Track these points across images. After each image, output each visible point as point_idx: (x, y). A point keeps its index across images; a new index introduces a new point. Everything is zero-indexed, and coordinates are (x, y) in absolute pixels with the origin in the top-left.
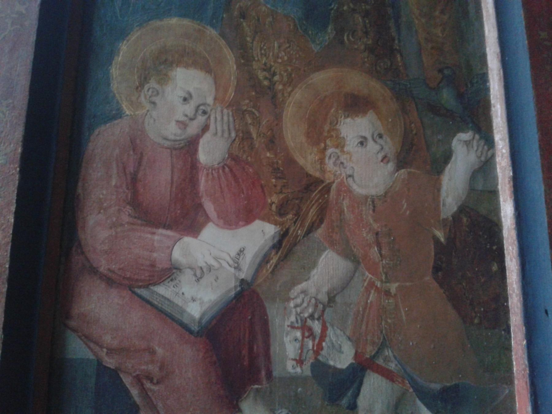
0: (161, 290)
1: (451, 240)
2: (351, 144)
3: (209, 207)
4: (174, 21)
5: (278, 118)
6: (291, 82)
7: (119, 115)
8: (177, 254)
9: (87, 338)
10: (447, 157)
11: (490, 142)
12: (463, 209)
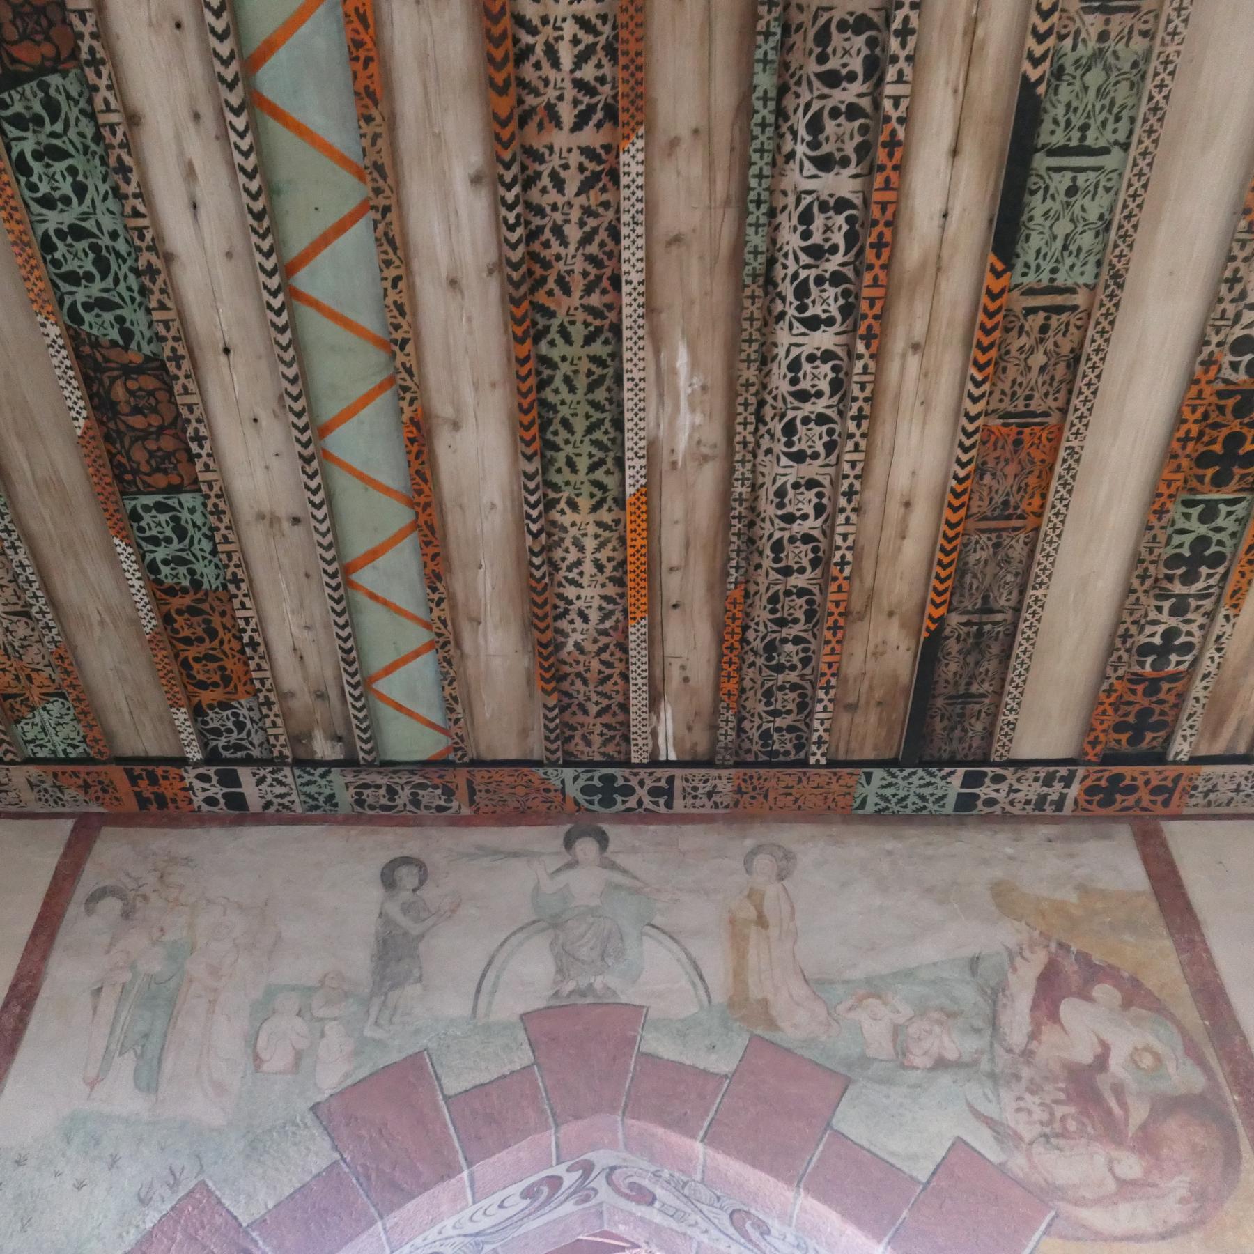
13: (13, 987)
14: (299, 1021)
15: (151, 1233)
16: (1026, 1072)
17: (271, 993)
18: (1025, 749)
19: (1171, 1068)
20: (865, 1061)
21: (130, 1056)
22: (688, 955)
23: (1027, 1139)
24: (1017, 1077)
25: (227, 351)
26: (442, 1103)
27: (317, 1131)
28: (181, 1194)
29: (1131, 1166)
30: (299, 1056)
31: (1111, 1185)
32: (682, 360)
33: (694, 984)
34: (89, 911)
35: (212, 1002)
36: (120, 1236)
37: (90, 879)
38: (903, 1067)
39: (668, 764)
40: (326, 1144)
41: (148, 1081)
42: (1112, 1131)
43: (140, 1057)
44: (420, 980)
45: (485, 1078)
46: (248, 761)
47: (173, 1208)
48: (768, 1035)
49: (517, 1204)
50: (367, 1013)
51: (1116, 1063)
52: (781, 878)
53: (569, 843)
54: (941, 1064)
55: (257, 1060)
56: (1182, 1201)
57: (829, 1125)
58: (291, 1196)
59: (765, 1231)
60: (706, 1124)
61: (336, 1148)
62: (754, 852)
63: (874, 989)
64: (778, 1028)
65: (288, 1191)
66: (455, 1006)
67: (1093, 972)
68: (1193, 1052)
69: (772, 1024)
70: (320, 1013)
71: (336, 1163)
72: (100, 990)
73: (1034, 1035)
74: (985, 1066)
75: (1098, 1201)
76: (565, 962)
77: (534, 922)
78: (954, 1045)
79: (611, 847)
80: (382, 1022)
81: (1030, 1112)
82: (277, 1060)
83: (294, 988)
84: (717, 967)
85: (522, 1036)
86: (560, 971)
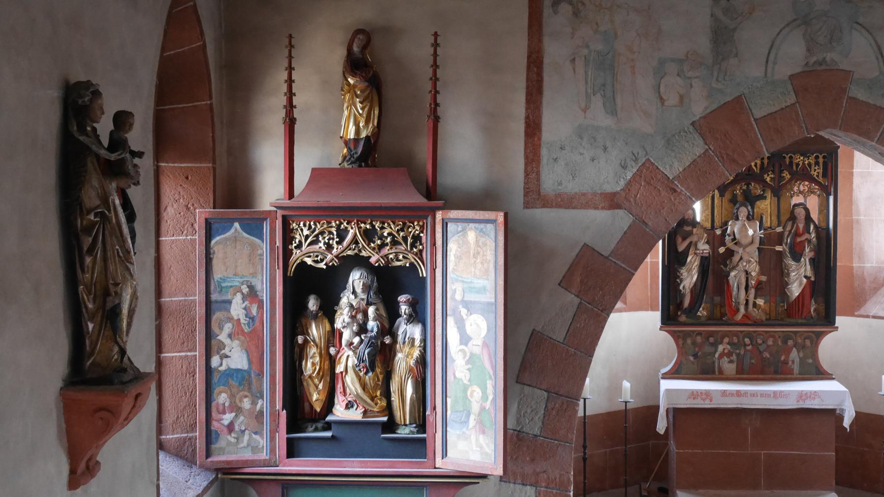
0: (222, 422)
1: (257, 414)
2: (245, 402)
3: (227, 411)
4: (221, 387)
5: (235, 400)
6: (237, 394)
7: (215, 400)
8: (223, 417)
9: (214, 427)
10: (258, 403)
11: (264, 401)
12: (259, 410)
13: (529, 57)
14: (678, 78)
15: (630, 181)
17: (662, 62)
21: (598, 95)
26: (754, 123)
27: (696, 136)
28: (640, 164)
30: (681, 97)
33: (877, 58)
34: (556, 12)
35: (633, 67)
36: (617, 182)
40: (701, 142)
41: (612, 111)
43: (604, 96)
44: (736, 55)
45: (774, 109)
47: (638, 170)
50: (712, 75)
58: (689, 166)
60: (879, 135)
61: (706, 144)
65: (687, 164)
66: (758, 72)
70: (690, 74)
71: (707, 150)
72: (574, 59)
77: (795, 20)
80: (720, 79)
83: (673, 60)
85: (790, 88)
86: (808, 50)
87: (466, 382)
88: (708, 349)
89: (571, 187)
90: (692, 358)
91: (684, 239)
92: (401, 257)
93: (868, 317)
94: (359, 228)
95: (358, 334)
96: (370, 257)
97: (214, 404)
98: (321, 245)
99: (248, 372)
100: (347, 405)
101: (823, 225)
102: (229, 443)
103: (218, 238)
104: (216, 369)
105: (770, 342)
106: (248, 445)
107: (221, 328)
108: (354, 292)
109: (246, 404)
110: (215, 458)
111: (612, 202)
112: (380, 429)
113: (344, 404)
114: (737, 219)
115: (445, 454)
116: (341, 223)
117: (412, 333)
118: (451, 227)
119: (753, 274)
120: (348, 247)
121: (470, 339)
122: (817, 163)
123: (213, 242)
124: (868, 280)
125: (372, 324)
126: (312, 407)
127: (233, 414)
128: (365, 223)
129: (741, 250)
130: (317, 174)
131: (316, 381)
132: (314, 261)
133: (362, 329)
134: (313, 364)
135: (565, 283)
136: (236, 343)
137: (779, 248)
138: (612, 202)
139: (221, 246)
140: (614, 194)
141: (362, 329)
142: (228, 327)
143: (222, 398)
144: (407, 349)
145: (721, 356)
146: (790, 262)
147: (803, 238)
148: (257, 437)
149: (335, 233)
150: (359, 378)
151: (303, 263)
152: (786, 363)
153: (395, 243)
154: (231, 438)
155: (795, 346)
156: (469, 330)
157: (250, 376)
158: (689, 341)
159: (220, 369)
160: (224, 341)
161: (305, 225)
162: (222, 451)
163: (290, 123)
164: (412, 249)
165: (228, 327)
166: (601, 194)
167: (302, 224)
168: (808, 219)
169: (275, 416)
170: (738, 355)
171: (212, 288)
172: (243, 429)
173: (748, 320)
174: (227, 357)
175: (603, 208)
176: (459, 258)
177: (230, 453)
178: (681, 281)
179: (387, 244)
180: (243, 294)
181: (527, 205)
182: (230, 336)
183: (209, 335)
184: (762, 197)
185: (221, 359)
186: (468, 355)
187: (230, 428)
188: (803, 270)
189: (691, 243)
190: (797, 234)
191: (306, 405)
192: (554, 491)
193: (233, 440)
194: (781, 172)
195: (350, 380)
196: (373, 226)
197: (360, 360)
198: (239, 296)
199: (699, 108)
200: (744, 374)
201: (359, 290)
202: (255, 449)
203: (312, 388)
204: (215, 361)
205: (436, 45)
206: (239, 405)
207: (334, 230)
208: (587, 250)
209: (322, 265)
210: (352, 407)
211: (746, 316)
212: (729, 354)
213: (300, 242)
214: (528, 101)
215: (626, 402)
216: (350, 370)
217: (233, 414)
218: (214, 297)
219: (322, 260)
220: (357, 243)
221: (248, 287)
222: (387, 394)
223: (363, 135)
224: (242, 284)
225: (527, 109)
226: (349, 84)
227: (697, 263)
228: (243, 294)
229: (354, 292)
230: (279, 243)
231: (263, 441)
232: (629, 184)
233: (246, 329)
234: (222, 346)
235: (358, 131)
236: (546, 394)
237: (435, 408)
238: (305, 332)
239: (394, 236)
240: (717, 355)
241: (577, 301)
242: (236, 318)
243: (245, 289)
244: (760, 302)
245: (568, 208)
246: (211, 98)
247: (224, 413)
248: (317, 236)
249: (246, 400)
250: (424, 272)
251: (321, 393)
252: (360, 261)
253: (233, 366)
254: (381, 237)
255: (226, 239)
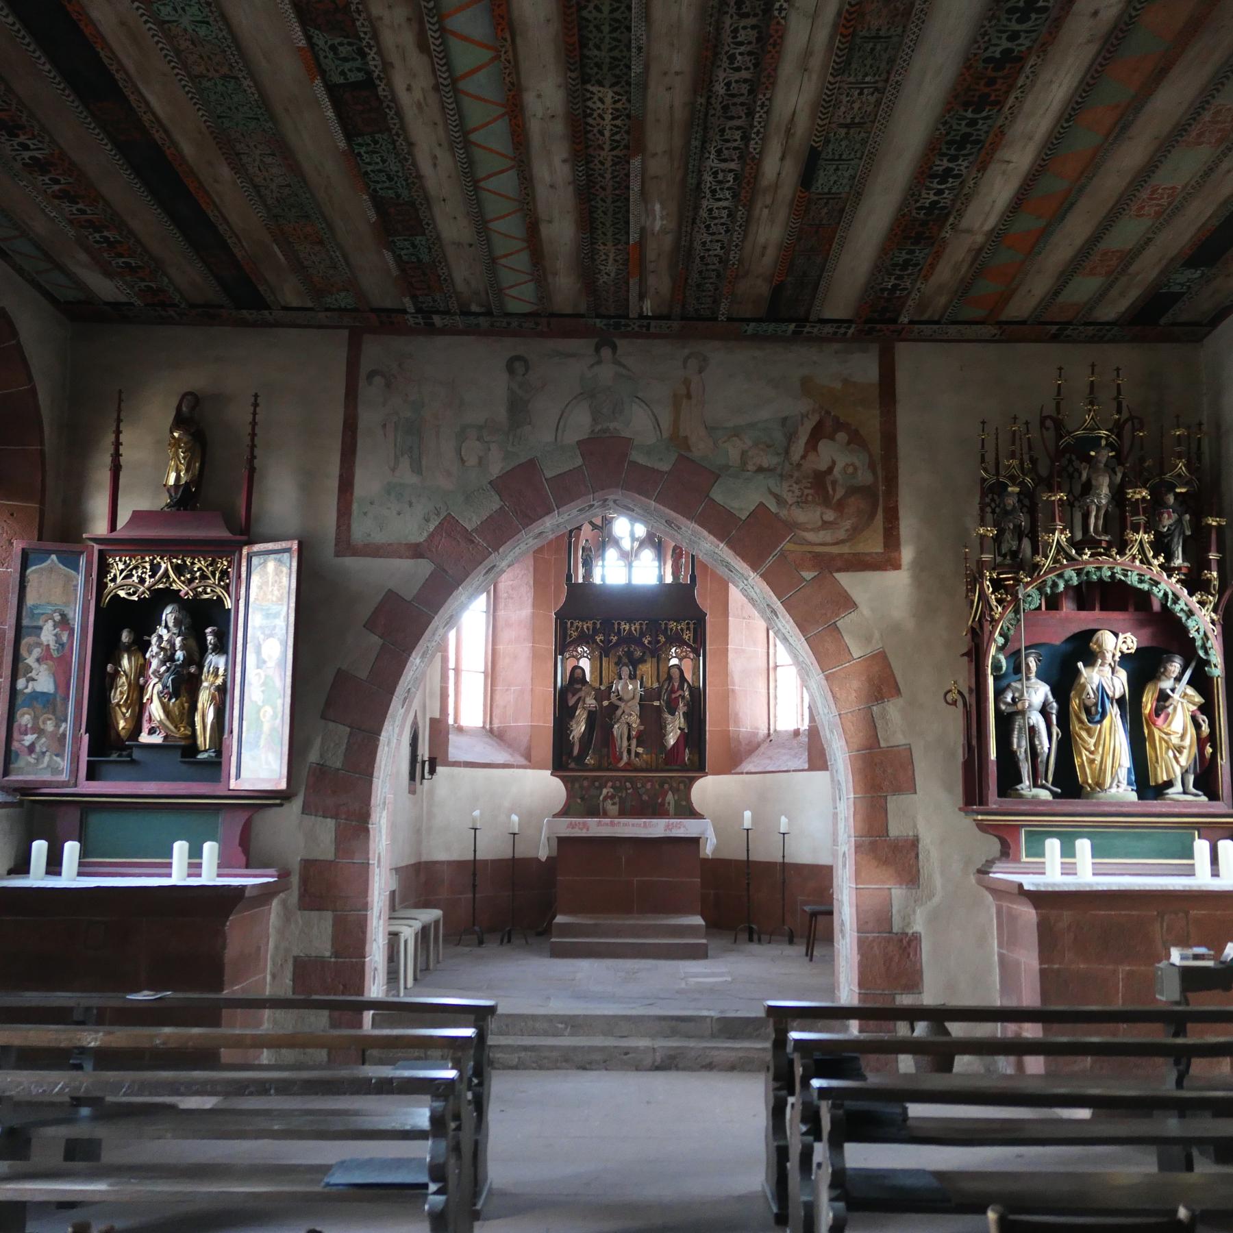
14: (477, 442)
16: (796, 474)
18: (827, 315)
19: (860, 473)
20: (727, 467)
21: (406, 456)
22: (652, 412)
23: (790, 502)
24: (791, 476)
25: (444, 200)
29: (830, 516)
30: (480, 459)
31: (820, 523)
32: (658, 207)
37: (365, 367)
38: (743, 470)
39: (647, 317)
40: (497, 498)
41: (417, 469)
42: (826, 501)
46: (437, 312)
48: (685, 454)
49: (575, 512)
51: (836, 470)
52: (700, 372)
53: (597, 349)
54: (760, 470)
55: (463, 461)
56: (847, 530)
57: (708, 496)
59: (680, 528)
62: (688, 357)
63: (736, 432)
64: (691, 451)
66: (548, 437)
67: (839, 426)
68: (872, 466)
69: (689, 449)
73: (804, 457)
74: (779, 471)
75: (812, 530)
76: (596, 416)
78: (767, 460)
79: (619, 352)
81: (793, 492)
82: (472, 461)
84: (666, 420)
85: (578, 452)
86: (594, 420)
87: (260, 703)
88: (593, 792)
89: (379, 538)
90: (579, 801)
91: (574, 695)
92: (209, 590)
93: (742, 773)
94: (171, 563)
95: (163, 663)
96: (180, 590)
97: (16, 725)
98: (135, 578)
99: (54, 695)
100: (150, 730)
101: (696, 685)
102: (28, 763)
103: (34, 568)
104: (21, 691)
105: (649, 785)
106: (48, 766)
107: (30, 652)
108: (166, 627)
109: (49, 726)
110: (12, 778)
111: (416, 551)
112: (179, 753)
113: (147, 731)
114: (621, 678)
115: (238, 776)
116: (155, 558)
117: (217, 663)
118: (255, 560)
119: (634, 725)
120: (159, 581)
121: (264, 662)
122: (688, 629)
123: (29, 571)
124: (743, 743)
125: (179, 655)
126: (118, 734)
127: (35, 736)
128: (177, 559)
129: (623, 705)
130: (137, 516)
131: (124, 710)
132: (129, 594)
133: (170, 658)
134: (121, 693)
135: (370, 625)
136: (44, 667)
137: (656, 703)
138: (416, 551)
139: (36, 575)
140: (418, 545)
141: (170, 658)
142: (37, 652)
143: (25, 719)
144: (211, 678)
145: (605, 798)
146: (669, 717)
147: (677, 694)
148: (58, 759)
149: (148, 567)
150: (165, 707)
151: (117, 596)
152: (662, 804)
153: (204, 577)
154: (31, 759)
155: (671, 788)
156: (264, 656)
157: (55, 699)
158: (577, 785)
159: (26, 691)
160: (31, 664)
161: (120, 560)
162: (20, 771)
163: (116, 469)
164: (219, 581)
165: (37, 652)
166: (406, 544)
167: (117, 559)
168: (682, 678)
169: (77, 740)
170: (620, 798)
171: (24, 614)
172: (44, 750)
173: (630, 767)
174: (34, 680)
175: (407, 557)
176: (260, 588)
177: (29, 774)
178: (571, 731)
179: (196, 578)
180: (54, 621)
181: (337, 554)
182: (38, 660)
183: (17, 658)
184: (642, 660)
185: (28, 681)
186: (263, 677)
187: (31, 749)
188: (677, 722)
189: (580, 698)
190: (673, 691)
191: (113, 734)
192: (354, 823)
193: (32, 761)
194: (657, 636)
195: (156, 710)
196: (184, 561)
197: (165, 687)
198: (50, 623)
199: (496, 469)
200: (625, 812)
201: (171, 624)
202: (56, 771)
203: (119, 715)
204: (21, 683)
205: (256, 405)
206: (42, 727)
207: (148, 566)
208: (391, 596)
209: (135, 598)
210: (155, 732)
211: (627, 764)
212: (612, 797)
213: (115, 575)
214: (342, 461)
215: (514, 834)
216: (155, 698)
217: (35, 736)
218: (25, 622)
219: (134, 593)
220: (168, 577)
221: (61, 615)
222: (192, 724)
223: (183, 482)
224: (55, 611)
225: (341, 469)
226: (174, 437)
227: (585, 716)
228: (54, 621)
229: (166, 627)
230: (94, 575)
231: (64, 764)
232: (432, 536)
233: (55, 654)
234: (29, 669)
235: (178, 478)
236: (348, 729)
237: (232, 732)
238: (118, 663)
239: (204, 571)
240: (601, 798)
241: (380, 641)
242: (45, 643)
243: (57, 617)
244: (640, 750)
245: (374, 556)
246: (42, 443)
247: (26, 734)
248: (131, 570)
249: (49, 722)
250: (229, 604)
251: (130, 721)
252: (169, 596)
253: (39, 689)
254: (192, 572)
255: (41, 569)
